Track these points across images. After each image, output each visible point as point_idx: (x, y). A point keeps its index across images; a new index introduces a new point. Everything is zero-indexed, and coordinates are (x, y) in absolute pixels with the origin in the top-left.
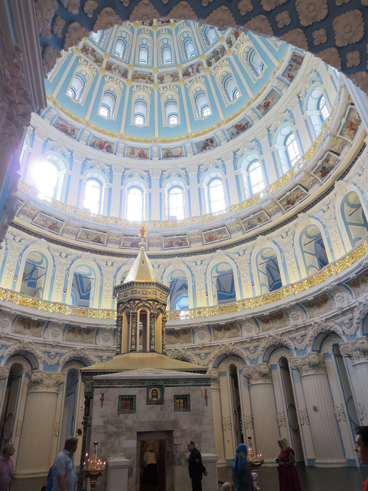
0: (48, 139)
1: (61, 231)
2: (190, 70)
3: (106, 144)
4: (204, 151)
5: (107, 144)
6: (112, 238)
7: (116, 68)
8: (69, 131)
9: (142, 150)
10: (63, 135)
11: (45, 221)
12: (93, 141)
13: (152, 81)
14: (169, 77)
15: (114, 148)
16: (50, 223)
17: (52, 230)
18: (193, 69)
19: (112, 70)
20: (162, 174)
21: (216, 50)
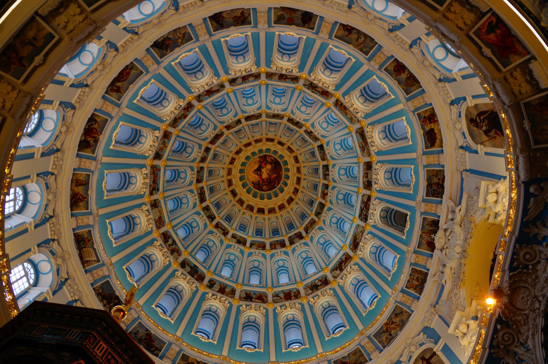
2: (170, 242)
4: (99, 298)
5: (92, 142)
8: (118, 84)
9: (84, 198)
12: (98, 120)
13: (151, 194)
14: (159, 215)
18: (172, 245)
20: (54, 240)
21: (198, 269)
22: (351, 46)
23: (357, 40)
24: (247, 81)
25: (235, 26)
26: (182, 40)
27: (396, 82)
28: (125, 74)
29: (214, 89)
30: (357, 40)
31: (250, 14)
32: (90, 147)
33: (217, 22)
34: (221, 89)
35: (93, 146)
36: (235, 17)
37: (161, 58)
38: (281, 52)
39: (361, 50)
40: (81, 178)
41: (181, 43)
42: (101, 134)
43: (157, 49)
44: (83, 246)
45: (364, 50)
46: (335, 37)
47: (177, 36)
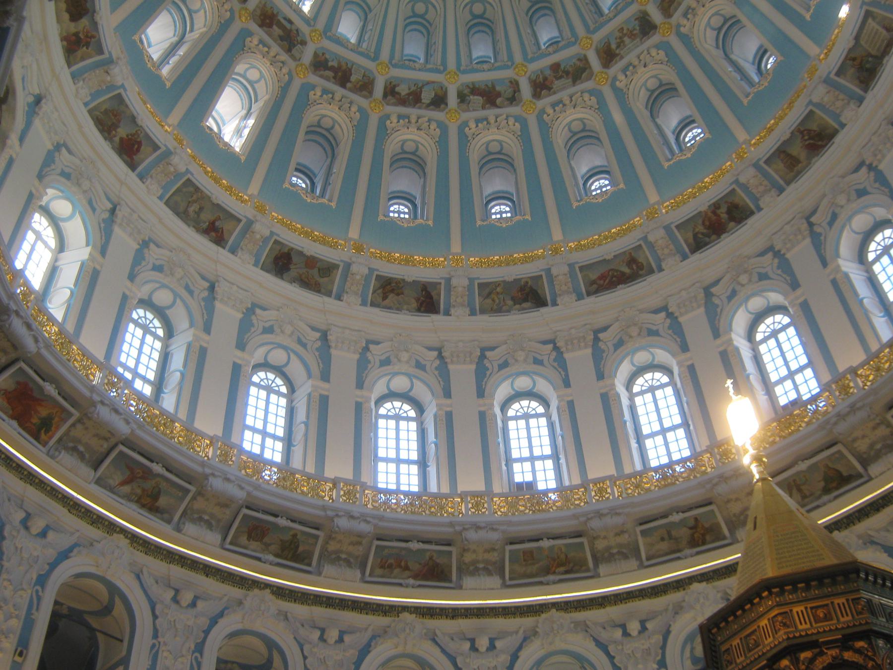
0: (596, 332)
1: (726, 531)
3: (718, 212)
6: (867, 441)
7: (620, 38)
8: (626, 270)
9: (802, 132)
10: (623, 294)
11: (666, 536)
12: (690, 235)
15: (743, 197)
16: (684, 533)
17: (704, 543)
19: (617, 52)
22: (215, 202)
23: (201, 209)
24: (413, 88)
25: (403, 280)
27: (139, 123)
28: (607, 281)
29: (478, 100)
30: (201, 209)
31: (374, 292)
32: (731, 203)
33: (429, 296)
34: (466, 91)
35: (726, 202)
36: (398, 295)
37: (541, 276)
38: (332, 134)
39: (197, 189)
40: (781, 166)
41: (499, 284)
42: (700, 212)
43: (539, 292)
44: (870, 59)
45: (192, 189)
46: (239, 221)
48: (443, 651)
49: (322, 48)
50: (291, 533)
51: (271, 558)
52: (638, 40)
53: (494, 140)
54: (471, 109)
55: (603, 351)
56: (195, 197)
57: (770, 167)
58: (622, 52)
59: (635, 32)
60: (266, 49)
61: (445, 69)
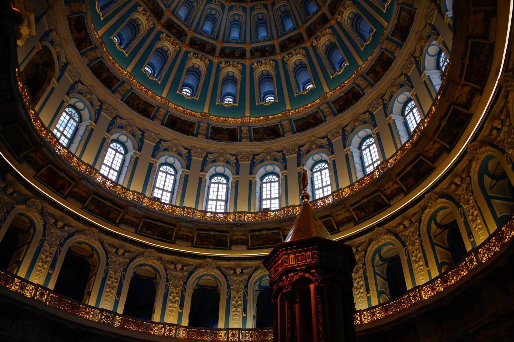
0: (299, 147)
6: (390, 190)
8: (312, 121)
12: (338, 106)
19: (314, 31)
22: (144, 100)
23: (139, 103)
24: (232, 50)
26: (260, 131)
27: (111, 70)
28: (305, 126)
30: (139, 103)
36: (220, 134)
39: (137, 96)
40: (372, 75)
45: (134, 96)
46: (155, 107)
47: (262, 134)
48: (223, 274)
49: (194, 36)
50: (163, 228)
51: (156, 237)
52: (322, 25)
53: (265, 70)
54: (255, 58)
55: (302, 155)
56: (136, 99)
57: (367, 76)
58: (315, 31)
59: (320, 22)
60: (169, 38)
61: (245, 42)
